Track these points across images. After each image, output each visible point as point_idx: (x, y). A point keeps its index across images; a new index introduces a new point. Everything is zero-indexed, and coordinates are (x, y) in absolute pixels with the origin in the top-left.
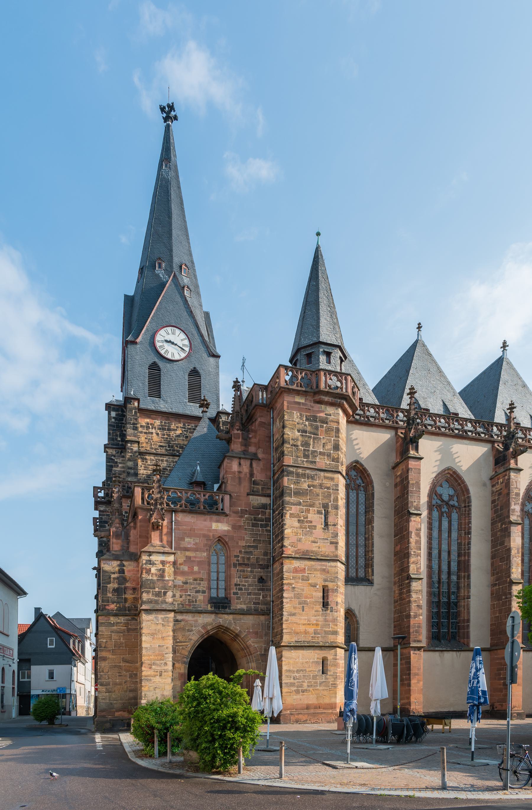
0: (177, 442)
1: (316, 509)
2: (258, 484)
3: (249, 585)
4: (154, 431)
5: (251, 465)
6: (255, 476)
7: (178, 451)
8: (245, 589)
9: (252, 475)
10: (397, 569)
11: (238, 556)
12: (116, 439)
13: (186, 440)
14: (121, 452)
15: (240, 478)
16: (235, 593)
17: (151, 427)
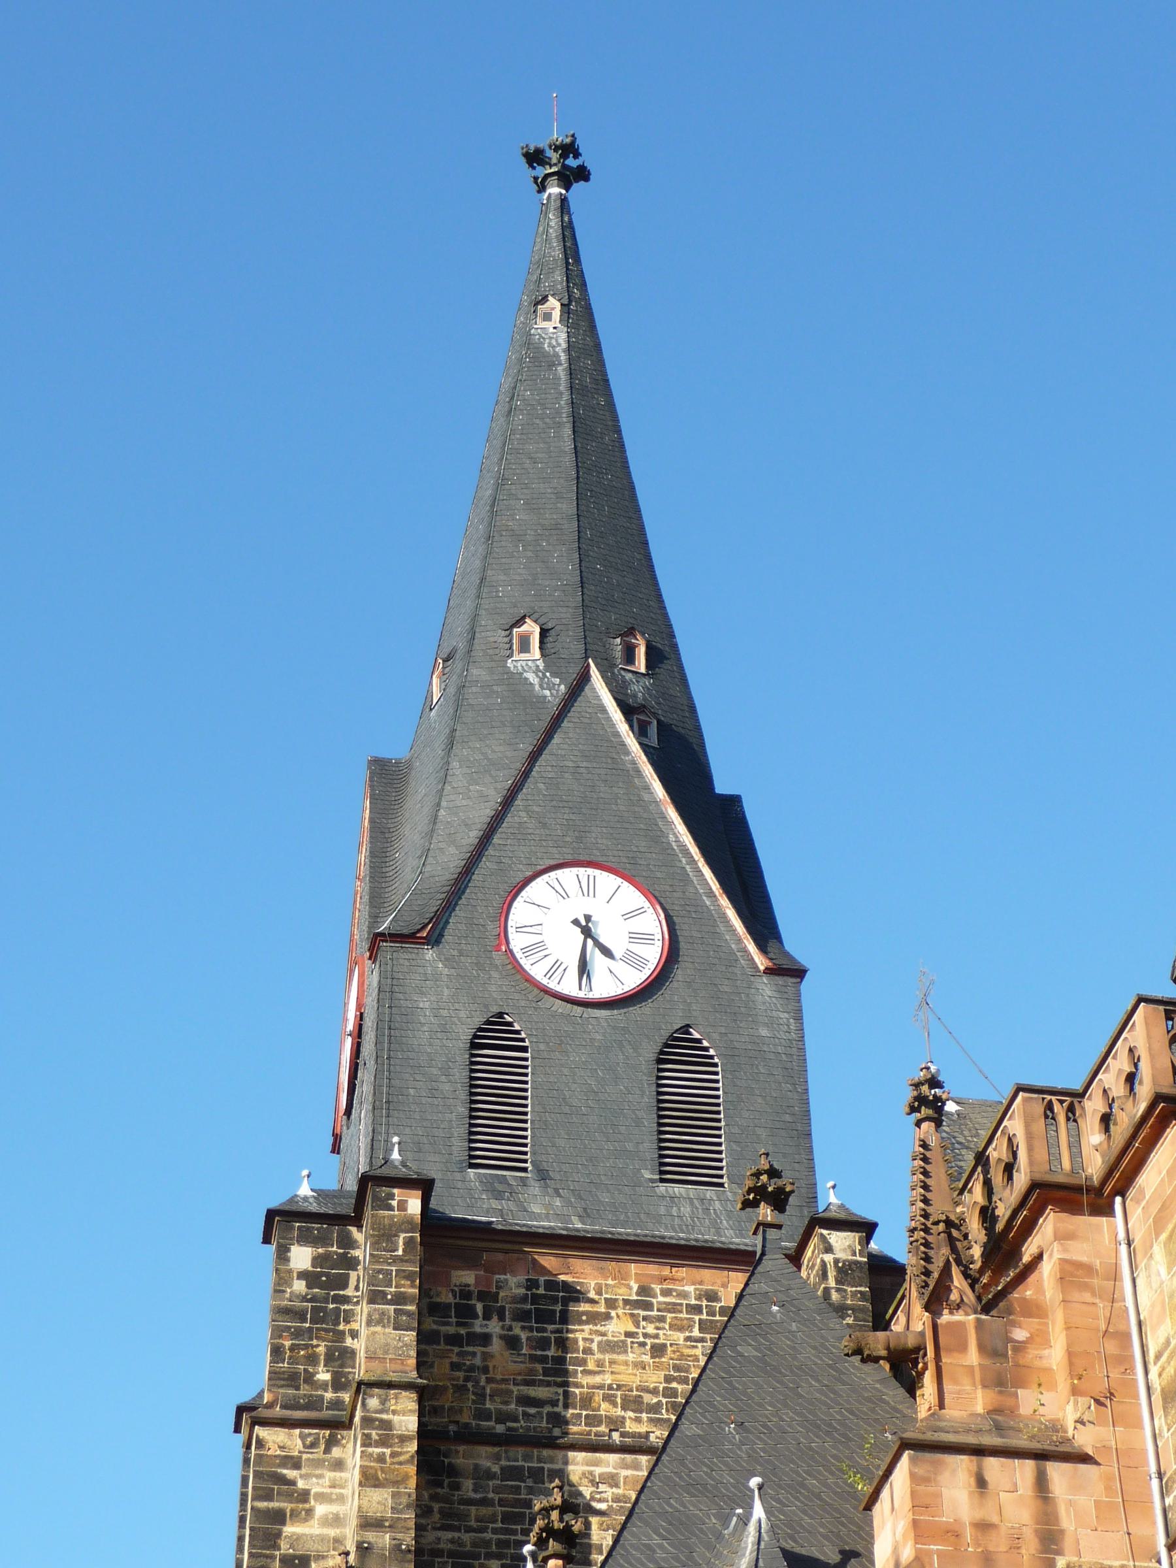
0: (608, 1379)
4: (494, 1327)
5: (1042, 1483)
6: (1068, 1543)
7: (616, 1424)
12: (309, 1379)
13: (657, 1367)
17: (479, 1307)
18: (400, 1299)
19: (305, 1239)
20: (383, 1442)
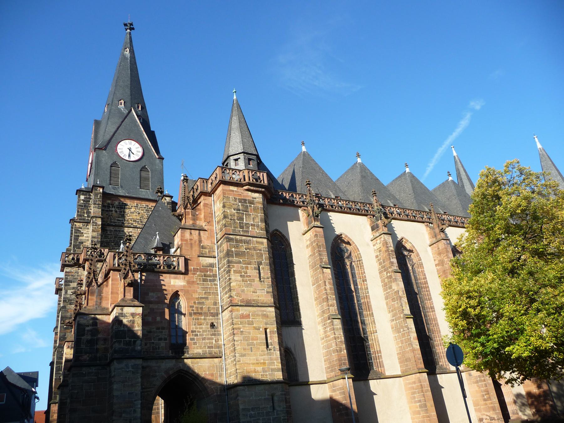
1: (253, 266)
2: (205, 248)
3: (203, 331)
4: (113, 209)
5: (199, 234)
7: (132, 224)
8: (200, 335)
9: (200, 241)
10: (320, 312)
11: (193, 307)
12: (83, 216)
14: (87, 225)
15: (191, 244)
16: (192, 339)
18: (98, 204)
19: (83, 194)
20: (96, 225)
